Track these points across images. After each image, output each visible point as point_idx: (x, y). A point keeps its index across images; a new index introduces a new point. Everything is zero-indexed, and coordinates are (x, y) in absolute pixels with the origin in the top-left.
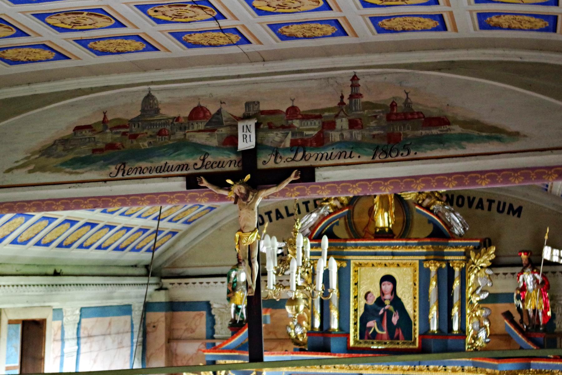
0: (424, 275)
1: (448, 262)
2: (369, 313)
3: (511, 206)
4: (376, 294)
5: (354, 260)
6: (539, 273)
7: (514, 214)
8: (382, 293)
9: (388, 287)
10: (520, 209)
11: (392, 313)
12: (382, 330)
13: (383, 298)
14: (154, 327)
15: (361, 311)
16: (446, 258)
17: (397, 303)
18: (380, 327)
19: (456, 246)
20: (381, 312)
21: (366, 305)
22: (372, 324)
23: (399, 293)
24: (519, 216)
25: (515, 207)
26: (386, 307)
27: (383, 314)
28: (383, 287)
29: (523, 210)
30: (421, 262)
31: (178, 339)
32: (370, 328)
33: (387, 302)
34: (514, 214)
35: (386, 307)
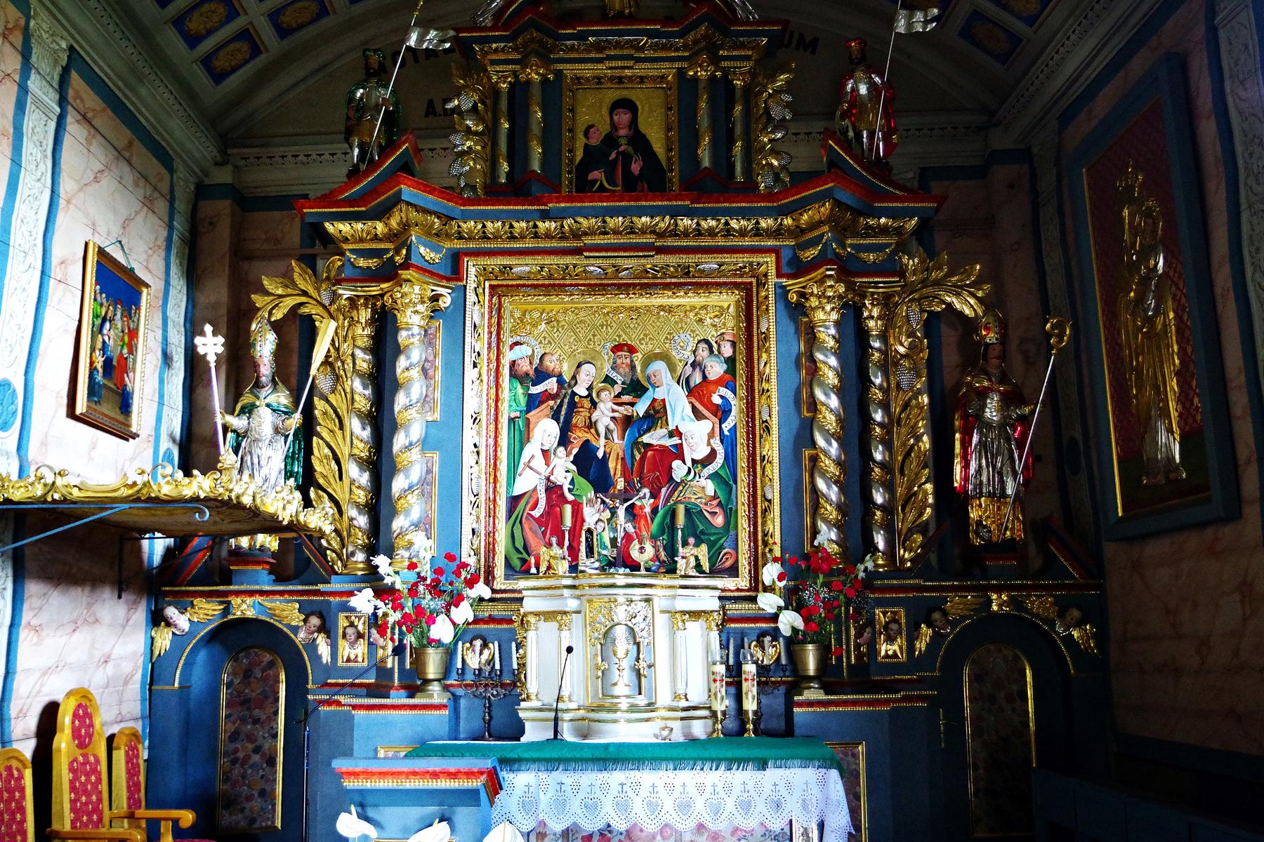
0: (687, 86)
1: (726, 72)
2: (594, 157)
3: (801, 37)
4: (605, 128)
5: (569, 70)
6: (881, 76)
7: (805, 50)
8: (614, 126)
9: (623, 117)
10: (815, 42)
12: (615, 185)
14: (211, 224)
15: (579, 155)
16: (725, 64)
17: (640, 142)
18: (612, 182)
19: (742, 46)
20: (613, 156)
21: (586, 147)
22: (597, 175)
23: (643, 127)
24: (813, 52)
25: (808, 38)
26: (622, 149)
27: (616, 159)
28: (616, 118)
30: (681, 73)
31: (249, 258)
32: (596, 181)
33: (623, 141)
34: (805, 50)
35: (622, 149)
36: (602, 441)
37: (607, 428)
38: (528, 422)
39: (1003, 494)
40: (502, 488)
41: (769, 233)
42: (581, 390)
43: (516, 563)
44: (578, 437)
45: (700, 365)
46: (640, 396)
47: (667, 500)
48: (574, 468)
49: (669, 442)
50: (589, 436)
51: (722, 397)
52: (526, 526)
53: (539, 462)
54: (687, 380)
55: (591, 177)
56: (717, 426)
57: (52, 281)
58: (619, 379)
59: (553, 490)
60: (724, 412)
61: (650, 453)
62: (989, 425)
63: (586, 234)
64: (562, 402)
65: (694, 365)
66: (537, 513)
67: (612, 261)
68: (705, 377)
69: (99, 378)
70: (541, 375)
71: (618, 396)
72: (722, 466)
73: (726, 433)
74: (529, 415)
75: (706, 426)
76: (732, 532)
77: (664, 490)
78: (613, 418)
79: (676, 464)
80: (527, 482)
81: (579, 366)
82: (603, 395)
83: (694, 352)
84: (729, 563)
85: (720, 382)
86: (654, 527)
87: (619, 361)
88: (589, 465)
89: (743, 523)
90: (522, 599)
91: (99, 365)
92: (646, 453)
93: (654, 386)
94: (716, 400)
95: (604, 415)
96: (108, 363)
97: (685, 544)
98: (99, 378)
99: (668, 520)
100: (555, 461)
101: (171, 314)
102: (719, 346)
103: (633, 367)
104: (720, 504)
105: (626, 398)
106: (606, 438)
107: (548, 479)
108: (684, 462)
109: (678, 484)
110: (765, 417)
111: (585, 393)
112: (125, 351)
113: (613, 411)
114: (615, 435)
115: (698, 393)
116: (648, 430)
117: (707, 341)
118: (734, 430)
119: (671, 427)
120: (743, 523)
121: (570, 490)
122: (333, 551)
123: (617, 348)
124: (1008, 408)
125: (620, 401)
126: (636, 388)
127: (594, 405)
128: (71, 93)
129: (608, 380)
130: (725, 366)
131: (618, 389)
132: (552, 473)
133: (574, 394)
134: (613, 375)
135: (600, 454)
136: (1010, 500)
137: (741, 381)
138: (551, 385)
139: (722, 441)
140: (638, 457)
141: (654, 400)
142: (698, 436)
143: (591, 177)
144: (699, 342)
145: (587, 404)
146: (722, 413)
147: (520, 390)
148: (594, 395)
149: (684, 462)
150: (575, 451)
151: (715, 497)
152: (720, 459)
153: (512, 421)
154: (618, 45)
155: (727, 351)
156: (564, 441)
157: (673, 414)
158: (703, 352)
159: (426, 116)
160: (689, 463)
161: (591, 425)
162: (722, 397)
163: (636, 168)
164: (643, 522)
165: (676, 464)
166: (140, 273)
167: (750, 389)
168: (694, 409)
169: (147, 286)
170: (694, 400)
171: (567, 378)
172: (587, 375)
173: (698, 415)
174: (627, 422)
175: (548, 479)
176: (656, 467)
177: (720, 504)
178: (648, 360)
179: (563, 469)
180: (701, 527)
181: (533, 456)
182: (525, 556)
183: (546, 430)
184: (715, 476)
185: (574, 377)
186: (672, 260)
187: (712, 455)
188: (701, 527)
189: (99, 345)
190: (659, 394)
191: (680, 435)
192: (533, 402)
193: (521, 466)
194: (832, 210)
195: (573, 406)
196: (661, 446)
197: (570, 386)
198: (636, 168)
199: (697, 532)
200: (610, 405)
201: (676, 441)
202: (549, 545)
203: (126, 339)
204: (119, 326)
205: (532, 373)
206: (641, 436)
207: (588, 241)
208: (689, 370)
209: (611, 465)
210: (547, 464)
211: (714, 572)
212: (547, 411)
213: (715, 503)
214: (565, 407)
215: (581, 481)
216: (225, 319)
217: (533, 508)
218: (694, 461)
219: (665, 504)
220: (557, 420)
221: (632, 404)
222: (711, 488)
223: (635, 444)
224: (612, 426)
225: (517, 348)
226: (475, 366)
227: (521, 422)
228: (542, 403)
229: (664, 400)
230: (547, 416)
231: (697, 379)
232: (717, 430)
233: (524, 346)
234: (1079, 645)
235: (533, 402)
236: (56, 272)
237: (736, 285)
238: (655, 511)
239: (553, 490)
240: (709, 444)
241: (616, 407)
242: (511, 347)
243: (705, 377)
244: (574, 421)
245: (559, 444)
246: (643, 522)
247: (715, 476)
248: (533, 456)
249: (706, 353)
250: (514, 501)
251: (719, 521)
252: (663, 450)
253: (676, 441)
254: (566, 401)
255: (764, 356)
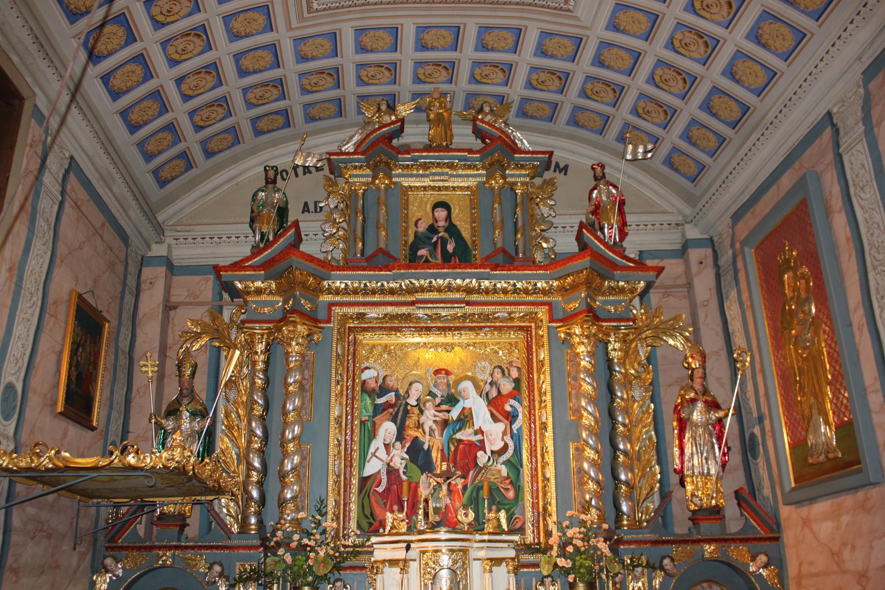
2: (420, 241)
3: (557, 164)
7: (560, 172)
9: (441, 213)
10: (566, 168)
11: (447, 241)
13: (436, 225)
15: (411, 238)
17: (452, 230)
20: (435, 239)
24: (565, 174)
25: (562, 166)
26: (440, 235)
27: (436, 242)
28: (436, 214)
29: (569, 168)
32: (422, 256)
33: (441, 230)
34: (560, 172)
35: (440, 235)
36: (427, 437)
37: (431, 428)
38: (374, 424)
39: (709, 473)
40: (355, 472)
41: (544, 292)
42: (412, 401)
43: (365, 526)
44: (412, 433)
45: (496, 383)
46: (454, 405)
47: (474, 479)
48: (407, 457)
49: (474, 438)
50: (417, 434)
51: (511, 406)
52: (372, 499)
53: (382, 453)
54: (487, 394)
55: (420, 253)
56: (508, 426)
57: (47, 315)
58: (439, 394)
59: (392, 472)
60: (513, 417)
61: (461, 446)
62: (697, 426)
63: (417, 292)
64: (399, 410)
65: (491, 384)
66: (380, 489)
67: (435, 311)
68: (499, 392)
69: (73, 387)
70: (383, 390)
71: (439, 405)
72: (513, 455)
73: (515, 432)
74: (375, 419)
75: (501, 426)
76: (520, 503)
77: (471, 473)
78: (435, 421)
79: (480, 454)
80: (372, 467)
81: (411, 384)
82: (428, 404)
83: (492, 375)
84: (518, 525)
85: (511, 396)
86: (465, 500)
87: (439, 381)
88: (418, 455)
89: (528, 497)
90: (372, 553)
91: (73, 378)
92: (458, 445)
93: (465, 399)
94: (508, 408)
95: (429, 417)
96: (79, 377)
97: (490, 510)
98: (73, 387)
99: (474, 494)
100: (394, 452)
101: (121, 345)
102: (509, 370)
103: (448, 385)
104: (511, 482)
105: (444, 407)
106: (430, 435)
107: (388, 465)
108: (485, 452)
109: (481, 469)
110: (544, 420)
111: (415, 403)
112: (91, 368)
113: (435, 416)
114: (436, 433)
115: (496, 404)
116: (460, 429)
117: (500, 367)
118: (520, 429)
119: (476, 427)
120: (528, 497)
121: (404, 473)
122: (231, 516)
123: (437, 372)
124: (709, 413)
125: (439, 409)
126: (452, 400)
127: (422, 412)
128: (69, 187)
129: (430, 393)
130: (513, 385)
131: (438, 401)
132: (391, 460)
133: (407, 404)
134: (435, 390)
135: (426, 447)
136: (714, 478)
137: (525, 394)
138: (391, 397)
139: (512, 437)
140: (453, 449)
141: (464, 408)
142: (495, 433)
143: (420, 253)
144: (495, 367)
145: (416, 411)
146: (511, 417)
147: (369, 401)
148: (421, 406)
149: (485, 452)
150: (407, 445)
151: (508, 478)
152: (511, 451)
153: (363, 423)
154: (438, 165)
155: (515, 374)
156: (400, 437)
157: (477, 418)
158: (498, 374)
159: (303, 212)
160: (489, 453)
161: (419, 426)
162: (511, 406)
163: (450, 247)
164: (456, 496)
165: (480, 454)
166: (105, 314)
167: (531, 401)
168: (492, 415)
169: (109, 322)
170: (492, 409)
171: (402, 392)
172: (417, 391)
173: (495, 419)
174: (445, 423)
175: (388, 465)
176: (465, 456)
177: (511, 482)
178: (458, 382)
179: (399, 458)
180: (498, 499)
181: (378, 449)
182: (371, 520)
183: (387, 429)
184: (508, 463)
185: (407, 392)
186: (477, 309)
187: (505, 448)
188: (498, 499)
189: (74, 364)
190: (467, 404)
191: (482, 433)
192: (378, 410)
193: (369, 456)
194: (588, 276)
195: (406, 412)
196: (469, 441)
197: (404, 398)
198: (450, 247)
199: (497, 501)
200: (433, 412)
201: (479, 437)
202: (392, 512)
203: (92, 359)
204: (88, 350)
205: (377, 389)
206: (454, 434)
207: (419, 296)
208: (488, 387)
209: (434, 454)
210: (388, 454)
211: (511, 532)
212: (388, 416)
213: (507, 482)
214: (401, 413)
215: (412, 466)
216: (158, 349)
217: (378, 486)
218: (493, 452)
219: (472, 483)
220: (395, 422)
221: (448, 411)
222: (504, 471)
223: (451, 439)
224: (434, 427)
225: (367, 371)
226: (338, 383)
227: (369, 424)
228: (383, 410)
229: (470, 409)
230: (388, 420)
231: (494, 393)
232: (508, 430)
233: (372, 370)
234: (766, 581)
235: (378, 410)
236: (50, 309)
237: (521, 328)
238: (465, 488)
239: (392, 472)
240: (503, 439)
241: (436, 413)
242: (363, 371)
243: (499, 392)
244: (407, 423)
245: (397, 440)
246: (456, 496)
247: (508, 463)
248: (378, 449)
249: (500, 375)
250: (364, 481)
251: (511, 494)
252: (471, 444)
253: (479, 437)
254: (402, 408)
255: (542, 377)
